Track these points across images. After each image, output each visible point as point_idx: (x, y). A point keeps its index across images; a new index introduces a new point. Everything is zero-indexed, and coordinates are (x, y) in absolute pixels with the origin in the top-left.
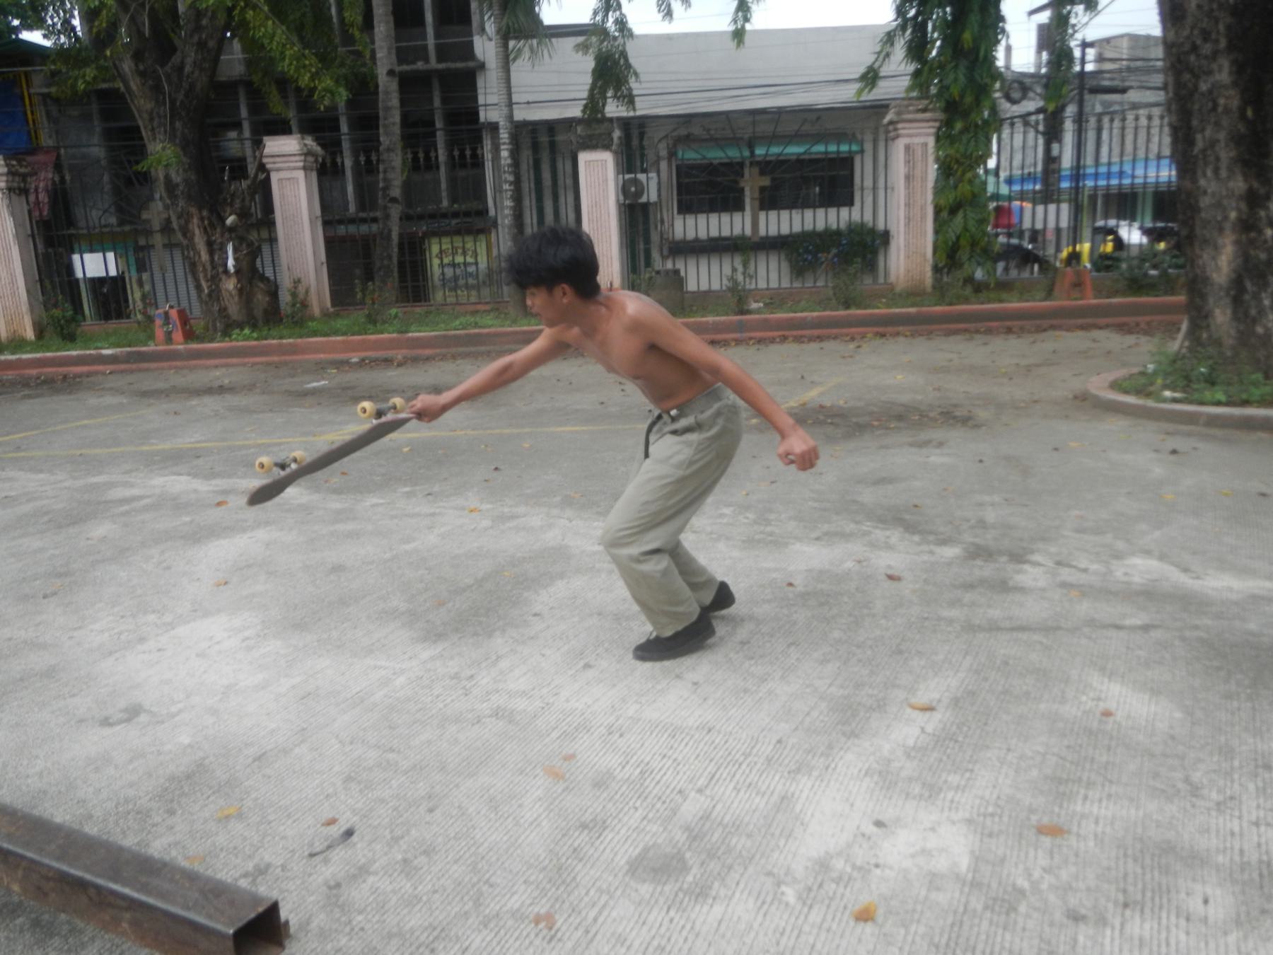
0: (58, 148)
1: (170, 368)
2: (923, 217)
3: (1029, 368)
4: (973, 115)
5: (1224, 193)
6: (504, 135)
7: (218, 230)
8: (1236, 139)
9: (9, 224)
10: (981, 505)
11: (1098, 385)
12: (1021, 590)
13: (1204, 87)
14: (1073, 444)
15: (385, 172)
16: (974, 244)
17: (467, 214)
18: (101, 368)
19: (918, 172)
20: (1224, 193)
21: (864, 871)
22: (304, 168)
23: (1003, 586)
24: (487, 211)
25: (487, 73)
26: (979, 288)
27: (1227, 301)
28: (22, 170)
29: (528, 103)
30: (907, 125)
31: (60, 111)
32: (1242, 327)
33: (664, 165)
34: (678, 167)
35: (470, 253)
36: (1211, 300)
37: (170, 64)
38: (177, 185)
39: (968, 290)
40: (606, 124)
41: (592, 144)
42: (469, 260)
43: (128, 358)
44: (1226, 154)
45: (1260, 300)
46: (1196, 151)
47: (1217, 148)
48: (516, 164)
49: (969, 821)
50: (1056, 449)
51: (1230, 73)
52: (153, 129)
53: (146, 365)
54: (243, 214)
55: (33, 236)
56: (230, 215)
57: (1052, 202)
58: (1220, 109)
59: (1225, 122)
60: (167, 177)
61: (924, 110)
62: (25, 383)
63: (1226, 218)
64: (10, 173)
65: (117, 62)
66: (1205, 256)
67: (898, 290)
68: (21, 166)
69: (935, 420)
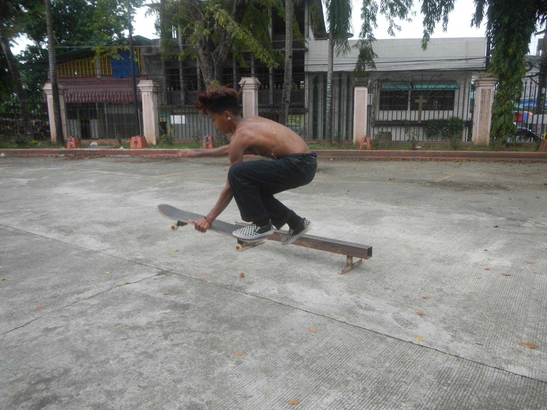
2: (487, 117)
3: (528, 175)
6: (329, 80)
9: (152, 104)
12: (525, 227)
15: (285, 92)
19: (486, 100)
21: (487, 265)
22: (255, 89)
23: (519, 226)
25: (309, 53)
26: (508, 145)
28: (157, 85)
29: (324, 65)
31: (150, 62)
37: (214, 52)
39: (504, 146)
40: (366, 77)
41: (359, 85)
42: (297, 124)
49: (511, 261)
55: (158, 108)
57: (541, 114)
61: (490, 77)
62: (162, 159)
64: (154, 86)
65: (197, 51)
67: (475, 144)
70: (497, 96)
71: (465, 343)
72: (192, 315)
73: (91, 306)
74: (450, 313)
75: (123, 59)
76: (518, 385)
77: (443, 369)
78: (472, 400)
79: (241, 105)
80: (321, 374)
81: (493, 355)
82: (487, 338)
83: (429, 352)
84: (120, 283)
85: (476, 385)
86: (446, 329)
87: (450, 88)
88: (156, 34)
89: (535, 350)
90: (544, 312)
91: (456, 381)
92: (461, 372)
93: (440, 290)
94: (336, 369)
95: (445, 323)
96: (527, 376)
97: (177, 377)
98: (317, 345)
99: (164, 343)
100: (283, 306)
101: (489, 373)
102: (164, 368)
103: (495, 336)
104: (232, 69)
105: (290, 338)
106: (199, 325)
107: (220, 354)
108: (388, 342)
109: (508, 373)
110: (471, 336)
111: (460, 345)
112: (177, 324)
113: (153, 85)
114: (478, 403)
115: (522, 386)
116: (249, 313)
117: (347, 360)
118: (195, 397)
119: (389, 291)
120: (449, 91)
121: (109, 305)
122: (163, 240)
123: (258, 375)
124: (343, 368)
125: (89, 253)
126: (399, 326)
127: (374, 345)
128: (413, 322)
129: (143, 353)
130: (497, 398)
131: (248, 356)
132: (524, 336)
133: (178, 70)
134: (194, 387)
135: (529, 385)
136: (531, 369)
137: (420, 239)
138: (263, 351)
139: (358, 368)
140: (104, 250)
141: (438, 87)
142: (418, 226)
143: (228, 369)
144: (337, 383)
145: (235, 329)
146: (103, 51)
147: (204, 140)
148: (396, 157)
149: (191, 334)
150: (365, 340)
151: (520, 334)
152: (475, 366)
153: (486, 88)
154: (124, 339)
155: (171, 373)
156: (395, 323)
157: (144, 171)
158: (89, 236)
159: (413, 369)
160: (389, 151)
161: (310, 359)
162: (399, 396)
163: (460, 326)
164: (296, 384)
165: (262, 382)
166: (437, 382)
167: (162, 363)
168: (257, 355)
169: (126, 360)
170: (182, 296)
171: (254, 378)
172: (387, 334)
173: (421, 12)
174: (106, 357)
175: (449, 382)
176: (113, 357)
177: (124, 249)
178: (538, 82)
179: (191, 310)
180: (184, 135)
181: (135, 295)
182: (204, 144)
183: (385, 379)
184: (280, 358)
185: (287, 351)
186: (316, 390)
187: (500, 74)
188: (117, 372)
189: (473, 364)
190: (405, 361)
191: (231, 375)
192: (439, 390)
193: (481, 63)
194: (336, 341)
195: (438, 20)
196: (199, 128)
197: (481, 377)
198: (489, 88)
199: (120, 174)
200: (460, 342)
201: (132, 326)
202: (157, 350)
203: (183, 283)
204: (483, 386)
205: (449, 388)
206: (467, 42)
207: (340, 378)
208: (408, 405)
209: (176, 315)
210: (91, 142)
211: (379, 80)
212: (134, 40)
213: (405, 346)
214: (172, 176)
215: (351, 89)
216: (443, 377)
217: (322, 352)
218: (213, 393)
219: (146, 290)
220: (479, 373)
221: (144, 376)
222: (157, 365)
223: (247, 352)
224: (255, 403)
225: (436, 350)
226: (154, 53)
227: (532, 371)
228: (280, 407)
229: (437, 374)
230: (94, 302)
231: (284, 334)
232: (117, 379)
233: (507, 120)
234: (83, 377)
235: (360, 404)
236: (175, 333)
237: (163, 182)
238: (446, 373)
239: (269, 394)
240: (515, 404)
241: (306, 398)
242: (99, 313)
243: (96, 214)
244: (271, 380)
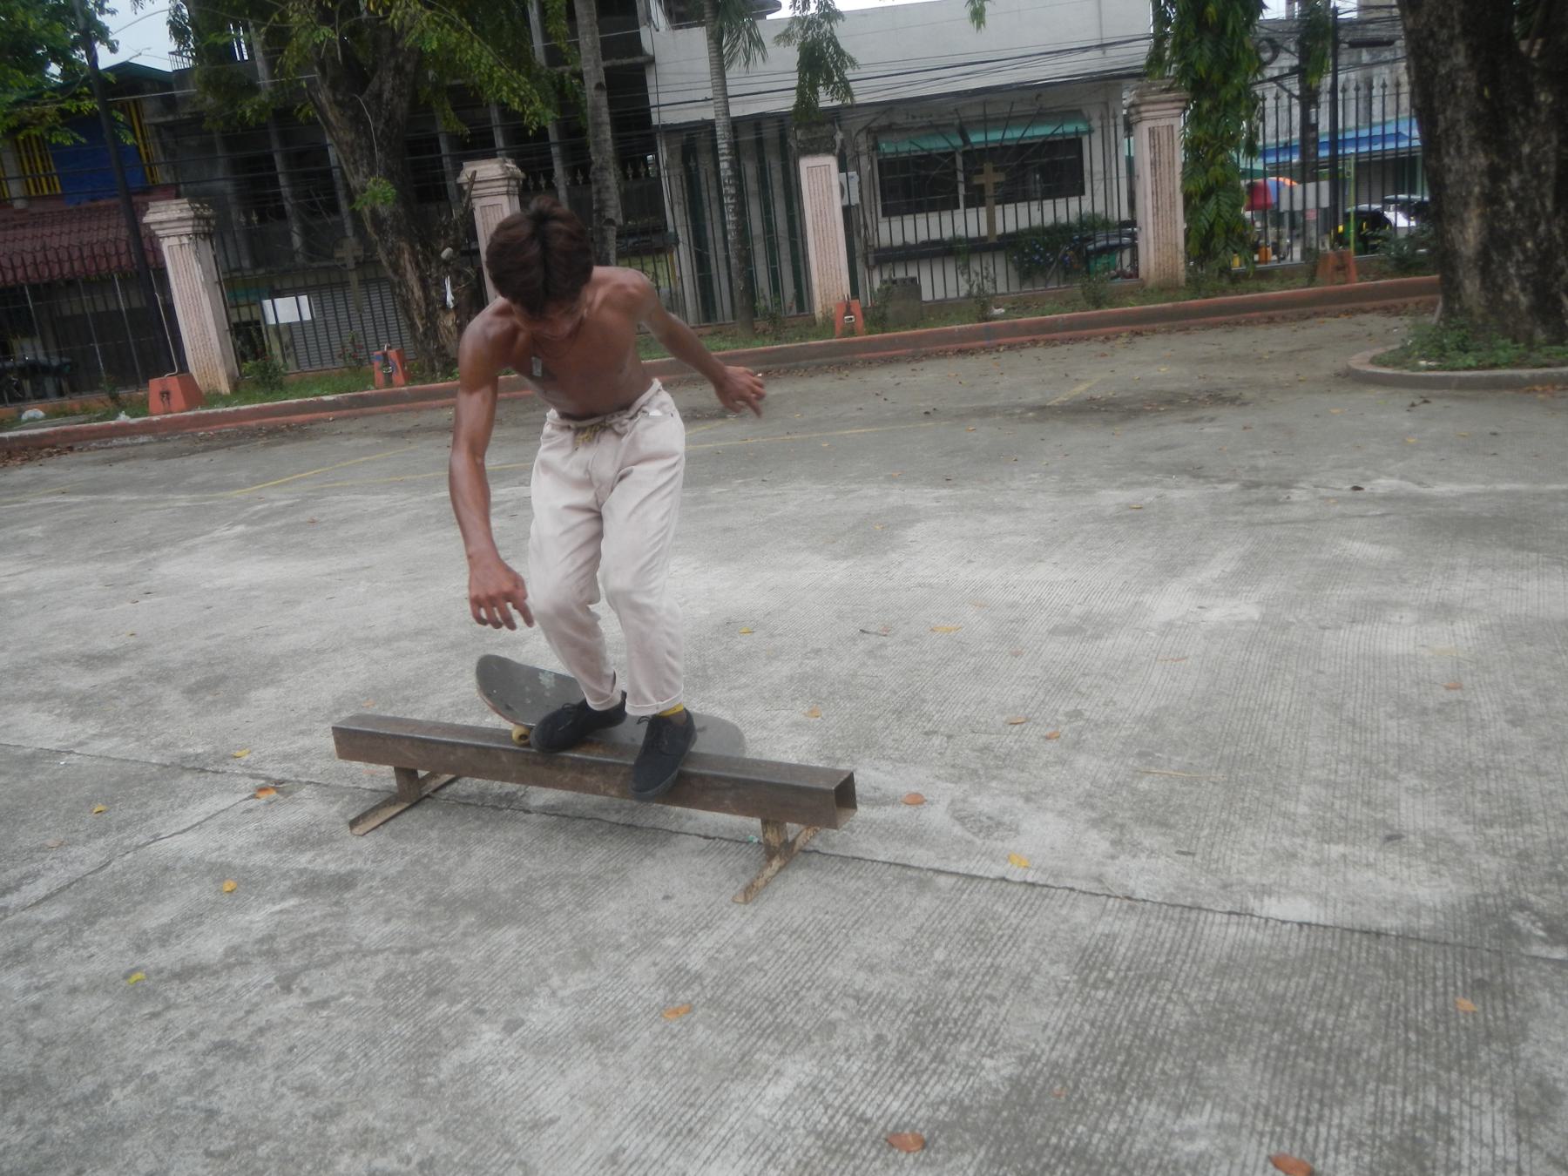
0: (177, 185)
1: (394, 411)
2: (1173, 206)
4: (1223, 93)
5: (1467, 169)
6: (723, 146)
7: (434, 264)
8: (1475, 118)
9: (197, 271)
10: (1253, 457)
11: (1359, 361)
13: (1443, 71)
14: (1334, 411)
15: (599, 192)
16: (1229, 230)
17: (644, 232)
18: (323, 415)
19: (1164, 159)
20: (1467, 169)
22: (508, 193)
23: (1275, 502)
24: (666, 230)
26: (1236, 278)
27: (1476, 272)
28: (206, 213)
29: (707, 100)
30: (1151, 107)
32: (1490, 296)
33: (864, 161)
34: (880, 164)
36: (1461, 273)
38: (385, 220)
39: (1225, 282)
40: (828, 126)
41: (813, 149)
44: (1466, 133)
45: (1506, 269)
46: (1438, 132)
47: (1458, 128)
48: (738, 175)
49: (1258, 603)
51: (1466, 57)
52: (355, 162)
53: (367, 410)
54: (455, 247)
58: (1459, 91)
59: (1464, 102)
60: (374, 212)
61: (1168, 90)
62: (253, 434)
63: (1470, 193)
64: (197, 217)
67: (1150, 284)
68: (204, 208)
69: (1202, 401)
70: (1192, 141)
71: (1149, 857)
72: (366, 903)
73: (45, 926)
74: (1105, 777)
75: (83, 140)
76: (1291, 953)
77: (1093, 942)
78: (1171, 1017)
79: (473, 247)
80: (755, 1016)
81: (1224, 876)
82: (1206, 832)
83: (1052, 898)
84: (135, 840)
85: (1180, 970)
86: (1095, 823)
87: (1064, 134)
88: (179, 53)
89: (1332, 846)
90: (1350, 734)
91: (1129, 969)
92: (1140, 940)
93: (1077, 714)
94: (797, 993)
95: (1093, 807)
96: (1314, 920)
97: (326, 1102)
98: (740, 932)
99: (282, 1005)
100: (638, 833)
101: (1215, 929)
102: (283, 1084)
103: (1224, 823)
104: (437, 140)
105: (662, 925)
106: (387, 929)
107: (454, 1010)
108: (939, 889)
109: (1263, 921)
110: (1164, 834)
111: (1134, 865)
112: (320, 939)
113: (192, 214)
114: (1188, 1023)
115: (1301, 952)
116: (536, 871)
117: (828, 961)
118: (384, 1154)
119: (936, 741)
120: (1061, 141)
121: (103, 915)
122: (267, 685)
123: (572, 1051)
124: (818, 988)
125: (33, 760)
126: (969, 836)
127: (901, 904)
128: (1007, 819)
129: (218, 1046)
130: (1239, 999)
131: (541, 1001)
132: (1303, 809)
133: (270, 158)
134: (378, 1124)
135: (1319, 945)
136: (1323, 899)
137: (1016, 577)
138: (585, 977)
139: (861, 976)
140: (81, 744)
141: (1029, 133)
142: (1006, 540)
143: (479, 1051)
144: (801, 1035)
145: (499, 926)
146: (12, 122)
147: (377, 364)
148: (940, 347)
149: (364, 964)
150: (876, 894)
151: (1291, 807)
152: (1177, 916)
154: (154, 1015)
155: (307, 1095)
156: (958, 830)
157: (198, 479)
158: (30, 706)
159: (1011, 955)
160: (918, 331)
161: (722, 978)
162: (977, 1040)
163: (1132, 810)
164: (685, 1057)
165: (583, 1071)
166: (1077, 982)
167: (278, 1067)
168: (566, 993)
169: (163, 1079)
170: (331, 850)
171: (560, 1062)
172: (936, 865)
174: (99, 1079)
175: (1110, 975)
176: (120, 1077)
177: (145, 733)
178: (1297, 93)
179: (360, 888)
180: (314, 354)
181: (184, 869)
182: (379, 376)
183: (936, 997)
184: (635, 990)
185: (655, 964)
186: (743, 1067)
187: (1193, 80)
188: (136, 1122)
189: (1170, 912)
190: (988, 937)
191: (490, 1068)
192: (1083, 1004)
193: (1139, 54)
194: (795, 911)
196: (357, 328)
197: (1195, 944)
199: (123, 498)
200: (1134, 856)
201: (178, 968)
202: (261, 1031)
203: (336, 808)
204: (1199, 970)
205: (1111, 993)
207: (810, 1018)
208: (1001, 1062)
209: (314, 912)
210: (21, 412)
211: (868, 130)
212: (112, 78)
213: (986, 892)
214: (286, 483)
215: (792, 164)
216: (1094, 963)
217: (755, 950)
218: (437, 1131)
219: (221, 847)
220: (1188, 934)
221: (221, 1120)
222: (263, 1078)
223: (536, 990)
224: (565, 1138)
225: (1072, 889)
226: (185, 112)
227: (1326, 906)
228: (640, 1137)
229: (1076, 960)
230: (56, 912)
231: (644, 914)
232: (136, 1143)
233: (1225, 208)
234: (26, 1156)
235: (868, 1084)
236: (316, 967)
237: (259, 507)
238: (1101, 951)
239: (606, 1103)
240: (1285, 1006)
241: (714, 1097)
242: (71, 945)
243: (52, 635)
244: (610, 1061)
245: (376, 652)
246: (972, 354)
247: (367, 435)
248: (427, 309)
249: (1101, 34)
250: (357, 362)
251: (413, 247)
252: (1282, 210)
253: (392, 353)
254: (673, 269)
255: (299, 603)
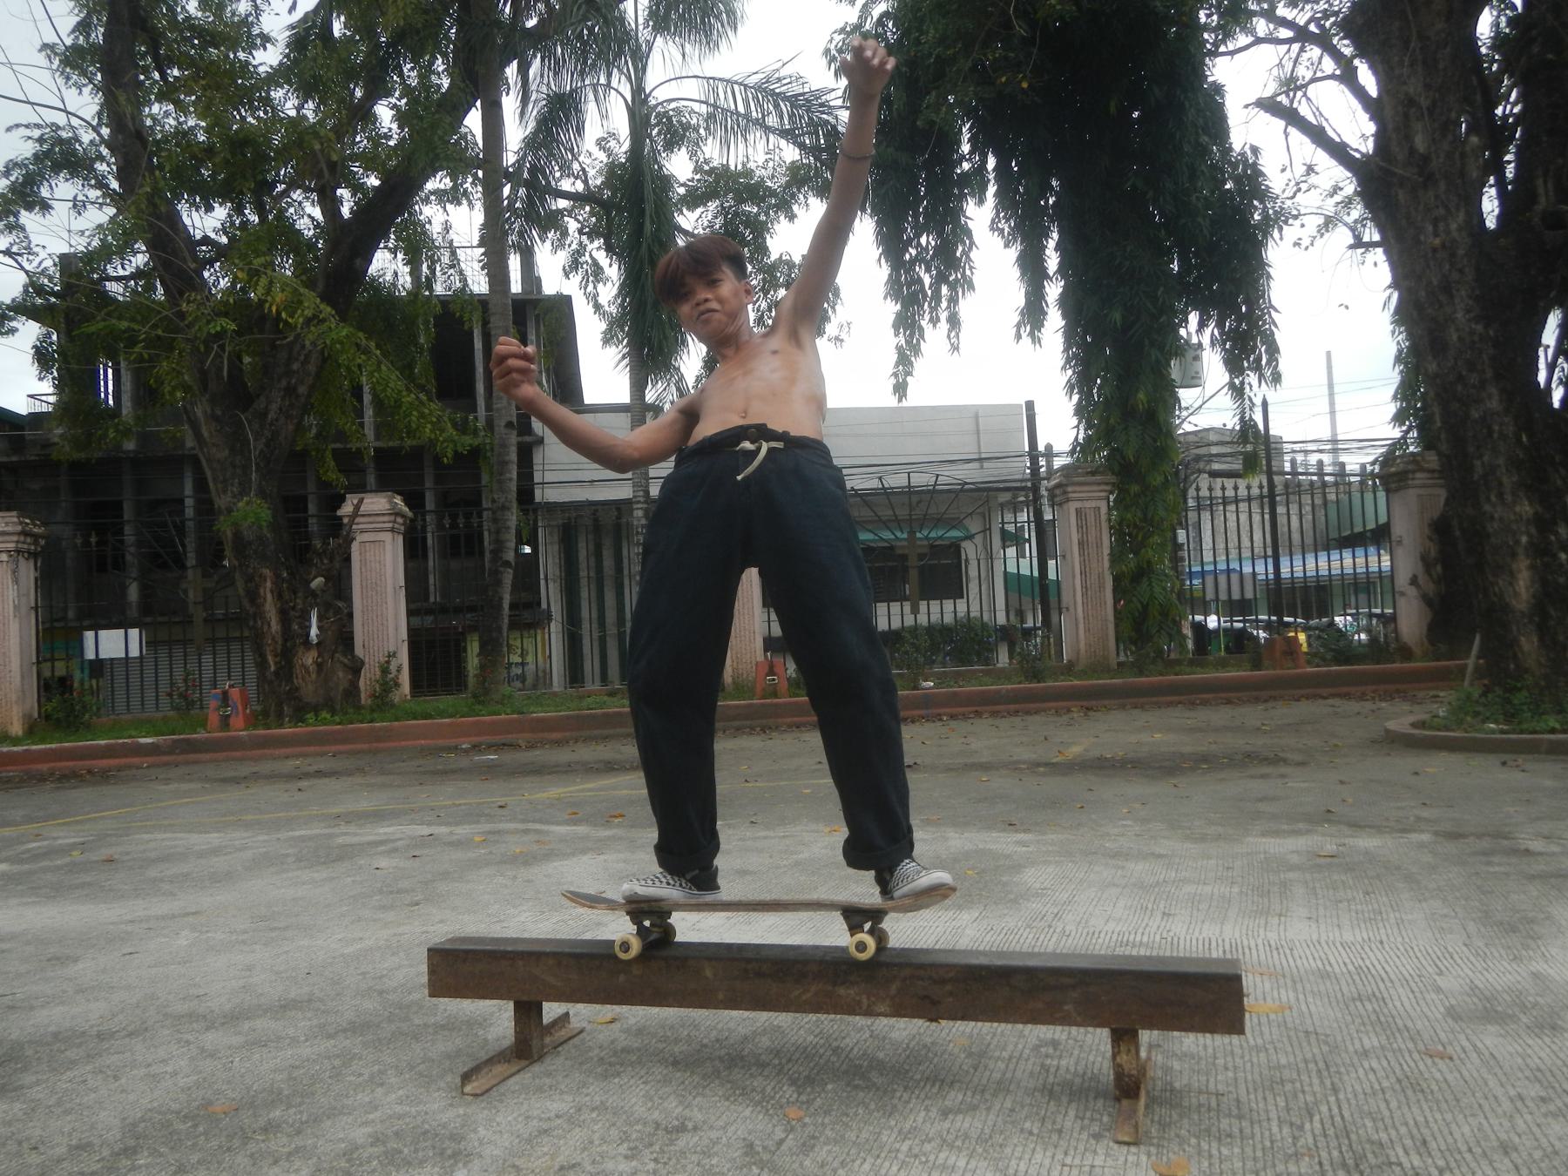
2: (1102, 587)
5: (1512, 517)
7: (300, 594)
9: (11, 593)
13: (1475, 414)
15: (498, 532)
18: (136, 760)
22: (392, 530)
24: (539, 604)
30: (1078, 489)
35: (519, 651)
36: (1514, 628)
43: (173, 749)
44: (1508, 481)
46: (1476, 477)
50: (1416, 773)
53: (192, 757)
56: (315, 577)
58: (1496, 435)
60: (237, 536)
61: (1093, 473)
62: (42, 779)
63: (1517, 542)
64: (24, 533)
66: (1501, 582)
68: (35, 525)
70: (1120, 524)
133: (118, 506)
142: (1189, 889)
147: (213, 703)
153: (1088, 504)
173: (885, 298)
182: (214, 719)
195: (935, 321)
198: (1093, 504)
206: (976, 415)
214: (77, 822)
226: (31, 455)
233: (1157, 589)
237: (34, 845)
245: (211, 1039)
246: (913, 722)
247: (191, 781)
248: (284, 645)
249: (979, 447)
250: (187, 705)
251: (277, 576)
252: (1208, 598)
253: (235, 693)
254: (544, 645)
255: (76, 960)
